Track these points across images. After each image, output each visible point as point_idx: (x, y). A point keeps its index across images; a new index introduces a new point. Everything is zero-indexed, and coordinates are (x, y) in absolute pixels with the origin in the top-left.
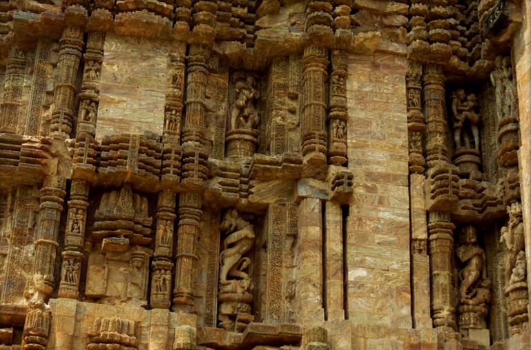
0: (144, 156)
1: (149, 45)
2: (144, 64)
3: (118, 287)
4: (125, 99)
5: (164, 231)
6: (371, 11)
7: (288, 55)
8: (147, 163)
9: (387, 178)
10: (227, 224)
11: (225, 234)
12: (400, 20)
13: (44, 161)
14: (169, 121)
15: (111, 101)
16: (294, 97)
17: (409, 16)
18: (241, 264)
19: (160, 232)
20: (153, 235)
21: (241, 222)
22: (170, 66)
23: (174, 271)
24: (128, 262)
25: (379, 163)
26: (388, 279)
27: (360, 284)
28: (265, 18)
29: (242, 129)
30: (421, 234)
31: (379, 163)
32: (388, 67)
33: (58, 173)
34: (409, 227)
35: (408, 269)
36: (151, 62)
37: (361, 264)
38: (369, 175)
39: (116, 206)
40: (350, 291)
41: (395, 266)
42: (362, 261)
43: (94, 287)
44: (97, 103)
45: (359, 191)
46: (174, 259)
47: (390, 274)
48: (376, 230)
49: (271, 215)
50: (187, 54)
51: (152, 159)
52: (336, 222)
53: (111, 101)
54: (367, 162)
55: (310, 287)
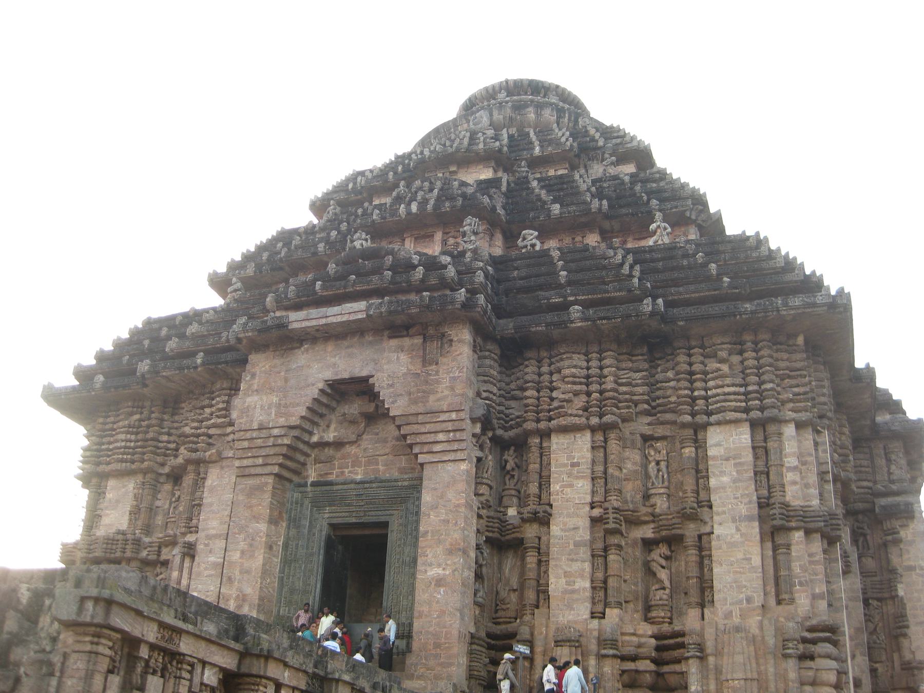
0: (105, 546)
6: (220, 435)
8: (106, 549)
9: (216, 536)
10: (155, 572)
15: (107, 515)
22: (134, 488)
25: (214, 528)
31: (214, 528)
32: (228, 466)
38: (209, 537)
41: (212, 589)
45: (200, 547)
48: (206, 569)
51: (110, 546)
54: (208, 529)
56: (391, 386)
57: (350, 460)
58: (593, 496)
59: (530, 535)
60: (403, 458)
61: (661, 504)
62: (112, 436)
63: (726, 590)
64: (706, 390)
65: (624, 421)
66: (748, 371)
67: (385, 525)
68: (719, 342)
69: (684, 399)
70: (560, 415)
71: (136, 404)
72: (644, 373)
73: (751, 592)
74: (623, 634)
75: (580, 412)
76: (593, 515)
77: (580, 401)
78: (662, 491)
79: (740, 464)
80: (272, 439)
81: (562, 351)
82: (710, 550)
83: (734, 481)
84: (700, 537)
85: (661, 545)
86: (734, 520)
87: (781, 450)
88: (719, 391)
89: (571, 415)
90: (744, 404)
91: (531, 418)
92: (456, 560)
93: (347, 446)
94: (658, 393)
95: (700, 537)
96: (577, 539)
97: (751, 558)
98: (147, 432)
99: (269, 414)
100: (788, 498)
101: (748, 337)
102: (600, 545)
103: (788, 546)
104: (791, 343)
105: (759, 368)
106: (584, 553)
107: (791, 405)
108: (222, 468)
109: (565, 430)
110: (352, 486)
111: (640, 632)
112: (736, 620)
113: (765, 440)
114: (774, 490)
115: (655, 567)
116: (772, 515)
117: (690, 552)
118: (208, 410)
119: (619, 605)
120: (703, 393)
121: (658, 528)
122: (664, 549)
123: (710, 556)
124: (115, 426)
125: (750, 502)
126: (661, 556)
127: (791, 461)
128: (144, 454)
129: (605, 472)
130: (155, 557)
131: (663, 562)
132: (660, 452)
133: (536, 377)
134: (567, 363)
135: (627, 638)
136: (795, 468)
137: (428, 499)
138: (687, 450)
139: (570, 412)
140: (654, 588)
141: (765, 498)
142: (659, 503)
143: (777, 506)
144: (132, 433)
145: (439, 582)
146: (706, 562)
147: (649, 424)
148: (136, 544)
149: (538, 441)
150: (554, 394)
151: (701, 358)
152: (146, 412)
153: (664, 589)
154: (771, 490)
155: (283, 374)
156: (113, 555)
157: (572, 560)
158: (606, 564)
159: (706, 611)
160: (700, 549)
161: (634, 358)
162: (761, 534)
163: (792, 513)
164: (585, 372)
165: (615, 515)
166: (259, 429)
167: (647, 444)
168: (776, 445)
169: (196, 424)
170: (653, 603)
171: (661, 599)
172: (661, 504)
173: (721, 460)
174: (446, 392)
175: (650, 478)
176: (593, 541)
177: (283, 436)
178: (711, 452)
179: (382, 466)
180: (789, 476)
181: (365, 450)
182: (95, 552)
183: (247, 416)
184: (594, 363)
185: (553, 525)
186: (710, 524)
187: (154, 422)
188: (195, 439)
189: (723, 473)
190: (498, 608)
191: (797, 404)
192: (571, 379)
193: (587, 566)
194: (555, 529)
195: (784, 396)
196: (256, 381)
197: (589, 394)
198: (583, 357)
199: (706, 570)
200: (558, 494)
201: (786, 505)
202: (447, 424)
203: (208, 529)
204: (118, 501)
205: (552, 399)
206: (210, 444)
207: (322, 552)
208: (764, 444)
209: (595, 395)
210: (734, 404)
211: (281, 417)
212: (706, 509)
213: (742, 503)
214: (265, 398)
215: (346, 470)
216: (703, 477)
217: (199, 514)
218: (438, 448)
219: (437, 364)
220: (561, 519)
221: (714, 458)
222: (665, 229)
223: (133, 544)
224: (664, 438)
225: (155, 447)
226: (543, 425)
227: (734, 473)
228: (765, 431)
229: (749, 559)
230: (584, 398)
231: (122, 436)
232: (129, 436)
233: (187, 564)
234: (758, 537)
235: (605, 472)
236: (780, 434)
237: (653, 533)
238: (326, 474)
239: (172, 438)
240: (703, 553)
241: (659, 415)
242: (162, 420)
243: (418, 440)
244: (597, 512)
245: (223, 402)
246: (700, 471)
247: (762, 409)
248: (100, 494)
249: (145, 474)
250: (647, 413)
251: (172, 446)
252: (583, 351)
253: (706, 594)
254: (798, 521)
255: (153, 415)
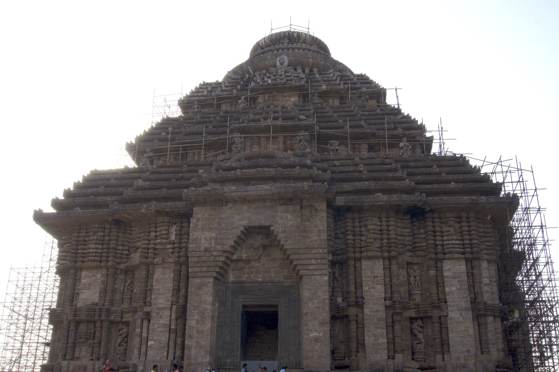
1: (95, 271)
2: (94, 278)
3: (83, 354)
4: (87, 291)
5: (98, 334)
7: (137, 267)
9: (163, 308)
10: (119, 328)
11: (119, 331)
12: (171, 250)
13: (62, 317)
14: (100, 296)
15: (83, 293)
16: (139, 282)
17: (173, 249)
18: (124, 341)
19: (96, 335)
20: (94, 336)
21: (124, 327)
22: (101, 277)
23: (100, 347)
24: (86, 345)
25: (161, 304)
26: (161, 344)
27: (151, 346)
28: (133, 254)
29: (127, 294)
30: (173, 327)
31: (161, 304)
32: (168, 267)
33: (67, 319)
34: (169, 325)
35: (168, 339)
36: (96, 277)
37: (152, 340)
39: (83, 328)
40: (148, 349)
41: (163, 339)
42: (153, 338)
43: (77, 355)
44: (79, 294)
46: (100, 344)
47: (162, 342)
48: (158, 327)
49: (130, 325)
50: (108, 272)
51: (90, 313)
52: (145, 326)
53: (83, 293)
54: (158, 304)
55: (135, 349)
56: (284, 232)
57: (254, 270)
58: (385, 294)
59: (352, 314)
60: (286, 270)
61: (418, 299)
62: (85, 245)
63: (456, 346)
64: (443, 241)
65: (400, 254)
66: (465, 233)
67: (276, 306)
68: (449, 216)
69: (432, 245)
70: (367, 251)
71: (101, 226)
72: (409, 230)
73: (469, 347)
74: (405, 367)
75: (379, 249)
76: (387, 304)
77: (377, 244)
78: (418, 292)
79: (462, 281)
80: (212, 257)
81: (367, 215)
82: (446, 324)
83: (458, 290)
84: (440, 317)
85: (418, 320)
86: (459, 310)
87: (480, 274)
88: (450, 242)
89: (374, 251)
90: (463, 250)
91: (351, 250)
92: (325, 329)
93: (252, 262)
94: (416, 240)
95: (440, 317)
96: (379, 317)
97: (468, 330)
98: (109, 244)
99: (211, 243)
100: (485, 299)
101: (464, 215)
102: (390, 320)
103: (486, 324)
104: (484, 218)
105: (470, 231)
106: (383, 324)
107: (485, 251)
108: (164, 268)
109: (369, 258)
110: (257, 284)
111: (413, 366)
112: (462, 361)
113: (472, 269)
114: (478, 295)
115: (416, 332)
116: (479, 309)
117: (436, 325)
118: (153, 234)
119: (402, 351)
120: (441, 243)
121: (418, 311)
122: (420, 322)
123: (447, 328)
124: (86, 239)
125: (467, 301)
126: (418, 326)
127: (486, 281)
128: (108, 257)
129: (391, 281)
130: (119, 319)
131: (421, 330)
132: (415, 271)
133: (352, 228)
134: (370, 222)
135: (407, 369)
136: (488, 284)
137: (307, 295)
138: (432, 272)
139: (373, 249)
140: (415, 343)
141: (473, 299)
142: (417, 298)
143: (482, 304)
144: (99, 244)
145: (317, 340)
146: (444, 330)
147: (410, 256)
148: (108, 312)
149: (353, 263)
150: (363, 238)
151: (439, 224)
152: (107, 231)
153: (420, 343)
154: (476, 295)
155: (217, 220)
156: (92, 318)
157: (377, 328)
158: (393, 330)
159: (445, 356)
160: (441, 324)
161: (404, 221)
162: (473, 317)
163: (488, 308)
164: (379, 228)
165: (400, 305)
166: (204, 251)
167: (409, 266)
168: (478, 272)
169: (147, 242)
170: (416, 351)
171: (420, 349)
172: (418, 299)
173: (451, 278)
174: (316, 238)
175: (411, 284)
176: (387, 317)
177: (219, 256)
178: (446, 274)
179: (273, 274)
180: (485, 288)
181: (263, 264)
182: (80, 316)
183: (197, 243)
184: (384, 223)
185: (365, 309)
186: (446, 311)
187: (114, 238)
188: (147, 251)
189: (452, 285)
190: (334, 352)
191: (489, 251)
192: (373, 231)
193: (385, 331)
194: (366, 311)
195: (482, 247)
196: (200, 223)
197: (382, 239)
198: (378, 220)
199: (444, 335)
200: (367, 292)
201: (485, 303)
202: (317, 255)
203: (158, 304)
204: (90, 285)
205: (361, 241)
206: (155, 254)
207: (240, 320)
208: (472, 271)
209: (385, 241)
210: (458, 249)
211: (218, 245)
212: (443, 303)
213: (462, 301)
214: (207, 233)
215: (252, 276)
216: (441, 287)
217: (151, 295)
218: (312, 267)
219: (309, 221)
220: (369, 306)
221: (447, 277)
222: (408, 146)
223: (105, 311)
224: (417, 264)
225: (114, 253)
226: (358, 255)
227: (458, 286)
228: (471, 264)
229: (468, 330)
230: (379, 241)
231: (94, 246)
232: (98, 246)
233: (145, 324)
234: (472, 320)
235: (391, 281)
236: (480, 266)
237: (415, 314)
238: (240, 277)
239: (125, 248)
240: (442, 326)
241: (416, 252)
242: (118, 237)
243: (300, 263)
244: (388, 303)
245: (165, 230)
246: (439, 282)
247: (472, 253)
248: (76, 280)
249: (108, 269)
250: (410, 251)
251: (126, 252)
252: (378, 216)
253: (444, 347)
254: (491, 312)
255: (112, 233)
